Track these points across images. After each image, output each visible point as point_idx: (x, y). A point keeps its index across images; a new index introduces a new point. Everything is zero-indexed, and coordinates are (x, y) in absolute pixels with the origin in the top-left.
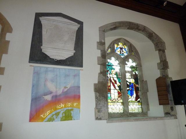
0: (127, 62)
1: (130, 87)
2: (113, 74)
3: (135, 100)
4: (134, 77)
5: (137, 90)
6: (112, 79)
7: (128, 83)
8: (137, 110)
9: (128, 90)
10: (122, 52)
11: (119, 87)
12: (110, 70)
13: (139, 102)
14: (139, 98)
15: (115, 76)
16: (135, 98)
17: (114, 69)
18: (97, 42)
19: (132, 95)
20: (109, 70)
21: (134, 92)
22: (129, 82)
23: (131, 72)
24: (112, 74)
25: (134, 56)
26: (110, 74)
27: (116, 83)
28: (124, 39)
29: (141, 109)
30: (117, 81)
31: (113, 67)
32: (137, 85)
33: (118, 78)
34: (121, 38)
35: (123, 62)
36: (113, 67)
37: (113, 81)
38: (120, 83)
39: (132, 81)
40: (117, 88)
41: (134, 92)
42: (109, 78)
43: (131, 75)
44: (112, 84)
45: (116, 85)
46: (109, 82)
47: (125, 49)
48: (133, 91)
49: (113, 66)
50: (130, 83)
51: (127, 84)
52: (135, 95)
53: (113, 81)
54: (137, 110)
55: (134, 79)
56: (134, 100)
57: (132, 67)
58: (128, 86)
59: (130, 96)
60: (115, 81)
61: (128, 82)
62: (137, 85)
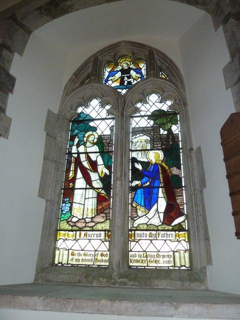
0: (139, 105)
1: (144, 180)
2: (88, 144)
3: (163, 223)
4: (162, 145)
5: (172, 187)
6: (83, 157)
7: (139, 167)
8: (166, 259)
9: (134, 189)
10: (126, 78)
11: (106, 180)
12: (81, 135)
13: (179, 228)
14: (181, 214)
15: (96, 148)
16: (162, 215)
17: (94, 129)
18: (21, 54)
19: (149, 203)
20: (76, 135)
21: (161, 194)
22: (142, 163)
23: (152, 132)
24: (85, 144)
25: (168, 81)
26: (78, 145)
27: (95, 170)
28: (129, 42)
29: (187, 255)
30: (100, 161)
31: (92, 124)
32: (175, 171)
33: (102, 153)
34: (120, 43)
35: (122, 110)
36: (92, 124)
37: (86, 164)
38: (108, 167)
39: (155, 156)
40: (97, 184)
41: (161, 194)
42: (76, 155)
43: (152, 141)
44: (79, 175)
45: (94, 176)
46: (72, 168)
47: (138, 71)
48: (155, 191)
49: (93, 120)
50: (145, 164)
51: (135, 170)
52: (162, 204)
53: (86, 164)
54: (166, 259)
55: (162, 149)
56: (156, 221)
57: (157, 116)
58: (136, 174)
59: (143, 209)
60: (94, 165)
61: (138, 162)
62: (175, 171)
